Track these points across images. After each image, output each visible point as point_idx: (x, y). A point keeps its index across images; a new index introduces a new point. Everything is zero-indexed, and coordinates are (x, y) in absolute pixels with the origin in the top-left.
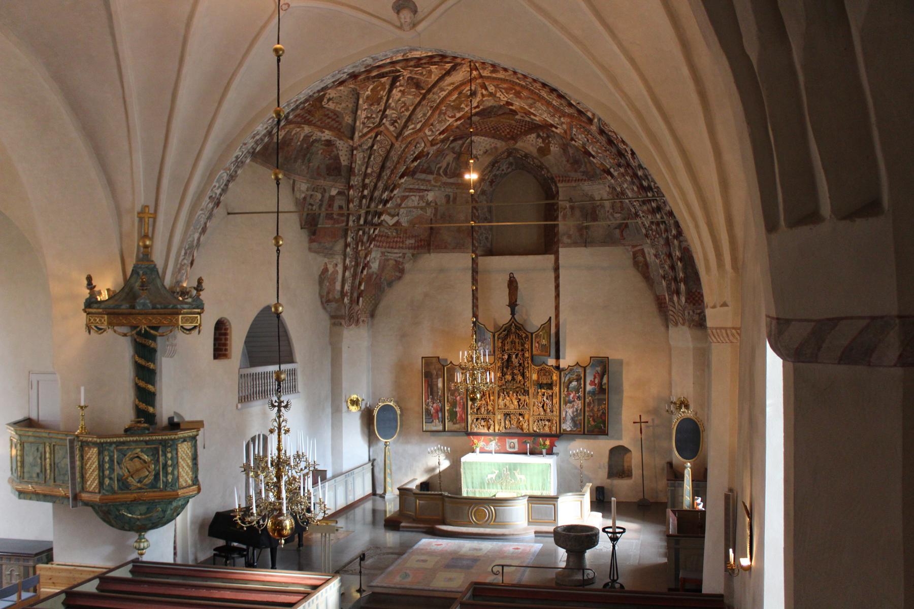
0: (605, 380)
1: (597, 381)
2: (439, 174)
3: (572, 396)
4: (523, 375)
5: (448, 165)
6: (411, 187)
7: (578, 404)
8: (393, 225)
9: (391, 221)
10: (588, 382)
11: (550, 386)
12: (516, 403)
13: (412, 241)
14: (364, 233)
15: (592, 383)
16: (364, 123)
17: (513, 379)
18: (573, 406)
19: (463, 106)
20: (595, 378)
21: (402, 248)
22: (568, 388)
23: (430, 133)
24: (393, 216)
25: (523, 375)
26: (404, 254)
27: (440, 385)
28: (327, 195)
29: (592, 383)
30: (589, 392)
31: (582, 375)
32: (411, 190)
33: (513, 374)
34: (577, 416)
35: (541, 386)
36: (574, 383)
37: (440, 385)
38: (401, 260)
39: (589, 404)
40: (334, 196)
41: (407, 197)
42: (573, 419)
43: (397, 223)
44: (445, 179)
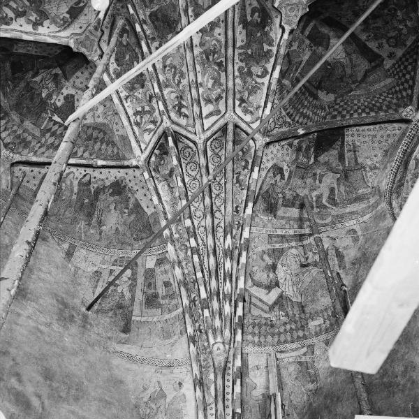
2: (320, 206)
5: (332, 190)
6: (279, 232)
8: (275, 303)
9: (273, 296)
13: (319, 321)
14: (213, 314)
16: (138, 124)
19: (266, 47)
21: (305, 337)
23: (248, 118)
24: (269, 288)
26: (311, 347)
28: (141, 271)
32: (283, 238)
38: (307, 359)
40: (152, 270)
41: (282, 251)
43: (281, 301)
44: (335, 211)
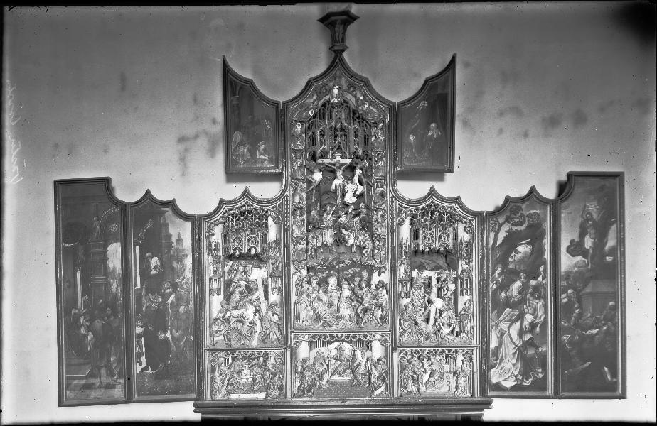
0: (611, 243)
1: (588, 243)
3: (517, 285)
4: (367, 226)
7: (540, 311)
10: (564, 244)
11: (448, 257)
12: (346, 311)
15: (576, 249)
17: (340, 240)
18: (521, 317)
20: (582, 235)
22: (505, 265)
25: (367, 226)
27: (115, 262)
29: (576, 249)
30: (569, 273)
31: (548, 226)
33: (339, 229)
34: (530, 344)
35: (419, 257)
36: (524, 249)
37: (115, 262)
39: (568, 308)
42: (521, 354)
